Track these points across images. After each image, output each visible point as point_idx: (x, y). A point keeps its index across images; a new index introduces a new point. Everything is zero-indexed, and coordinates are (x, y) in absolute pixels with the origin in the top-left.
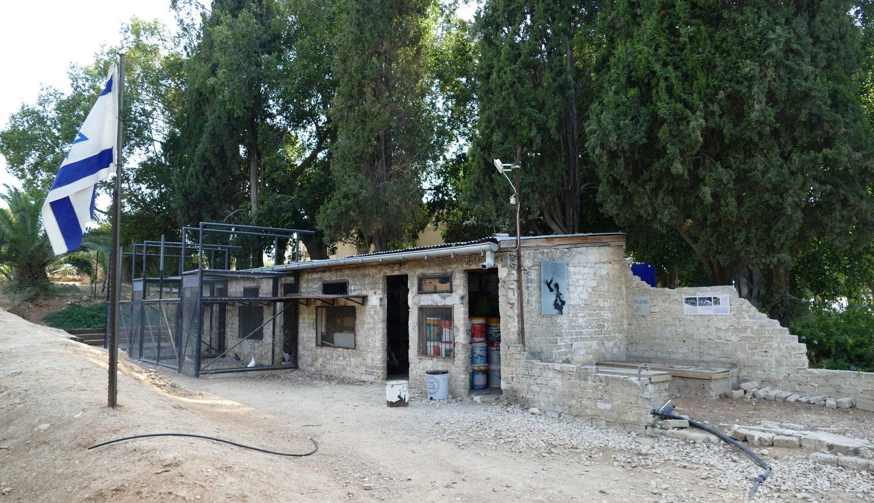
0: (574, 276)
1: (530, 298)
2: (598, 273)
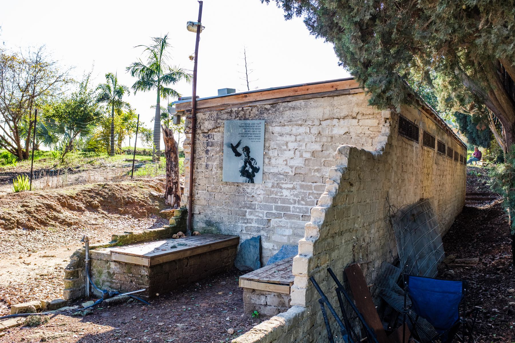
0: (279, 138)
1: (209, 163)
2: (326, 132)
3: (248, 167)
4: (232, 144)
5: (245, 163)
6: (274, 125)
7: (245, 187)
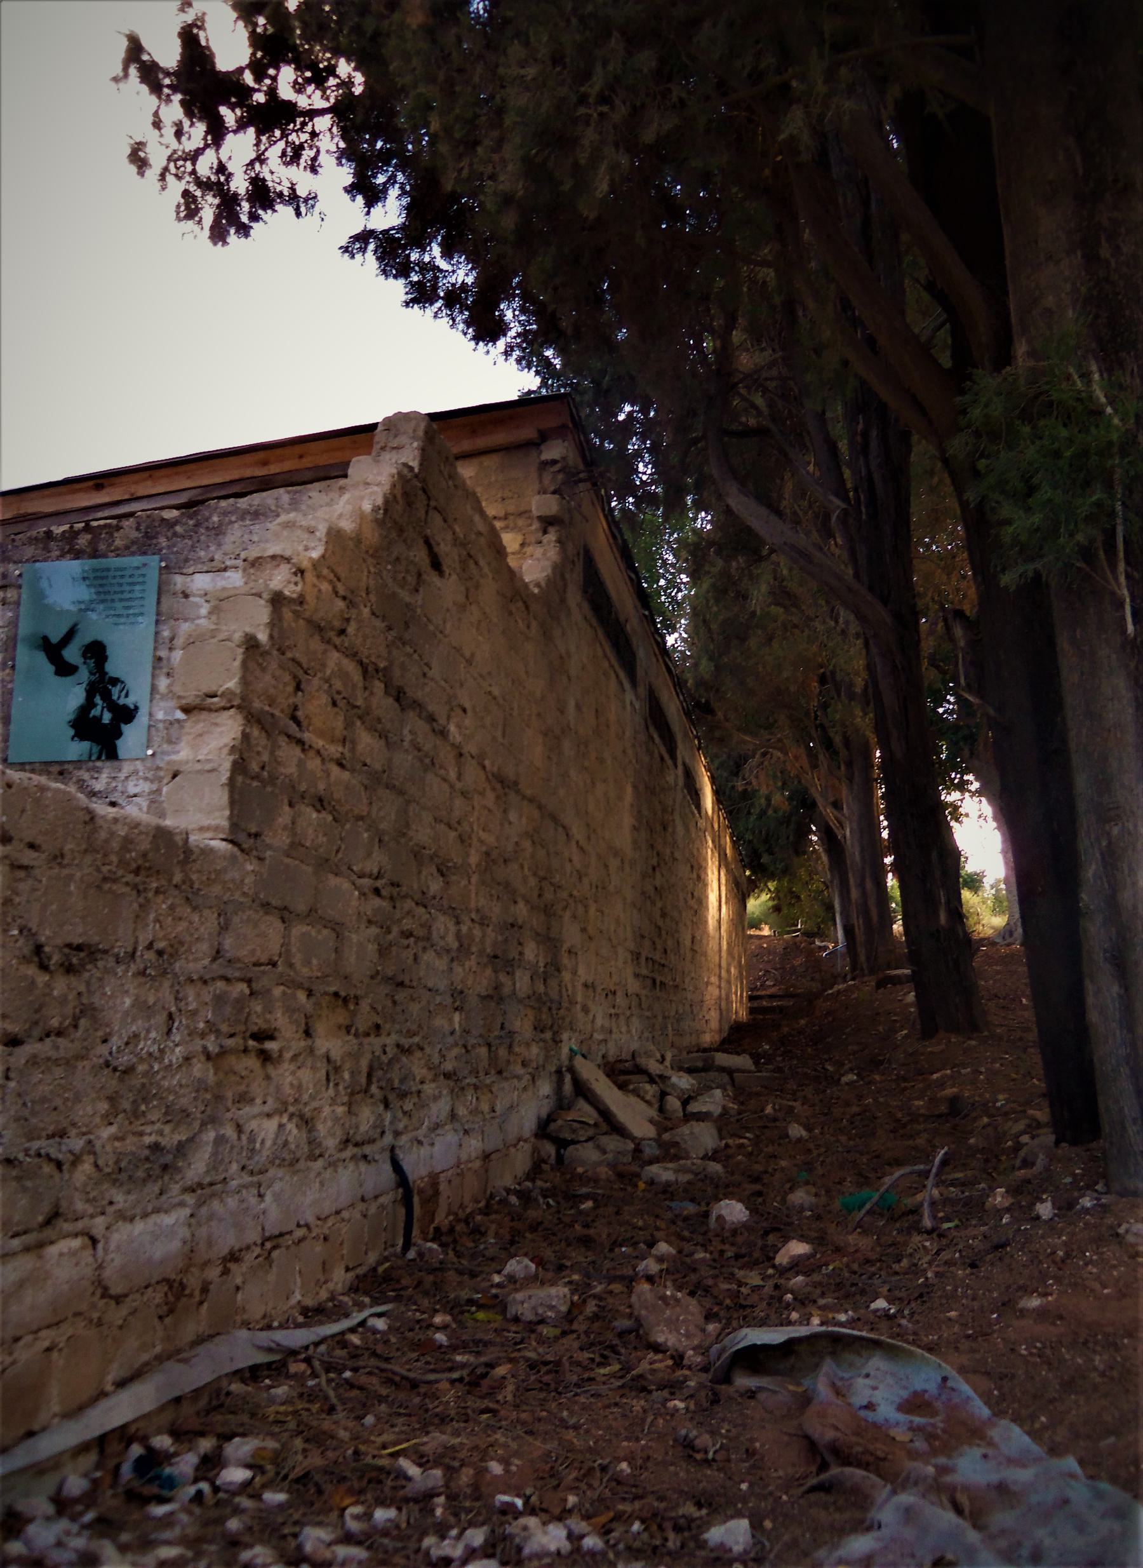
3: (99, 708)
4: (45, 639)
5: (91, 692)
6: (191, 570)
7: (86, 776)
